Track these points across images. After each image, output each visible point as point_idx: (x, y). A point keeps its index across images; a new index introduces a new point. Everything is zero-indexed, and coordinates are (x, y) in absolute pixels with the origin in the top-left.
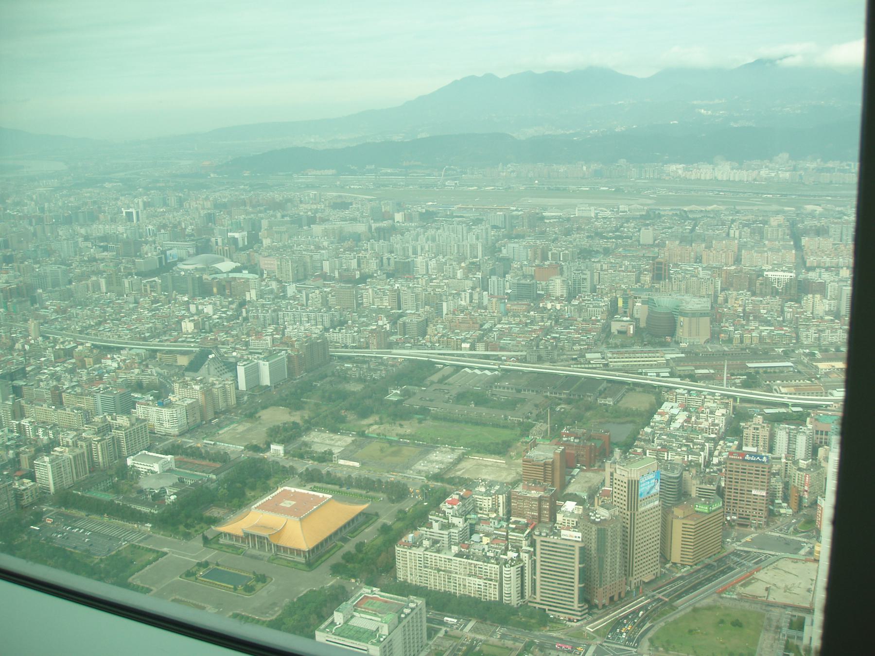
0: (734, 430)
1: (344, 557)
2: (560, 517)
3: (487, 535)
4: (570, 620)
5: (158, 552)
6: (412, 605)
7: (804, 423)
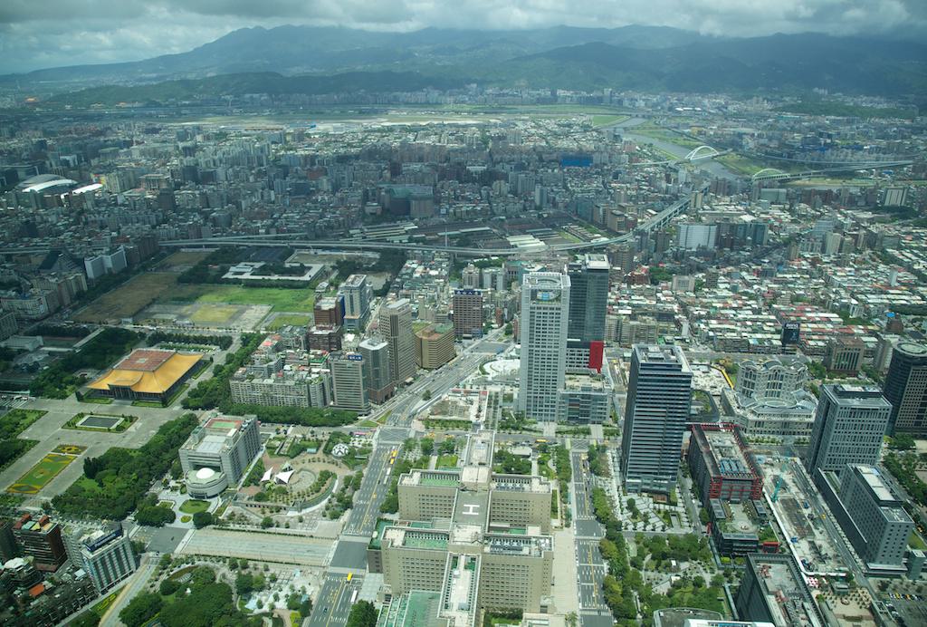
1: (189, 394)
3: (295, 364)
5: (39, 412)
7: (501, 266)
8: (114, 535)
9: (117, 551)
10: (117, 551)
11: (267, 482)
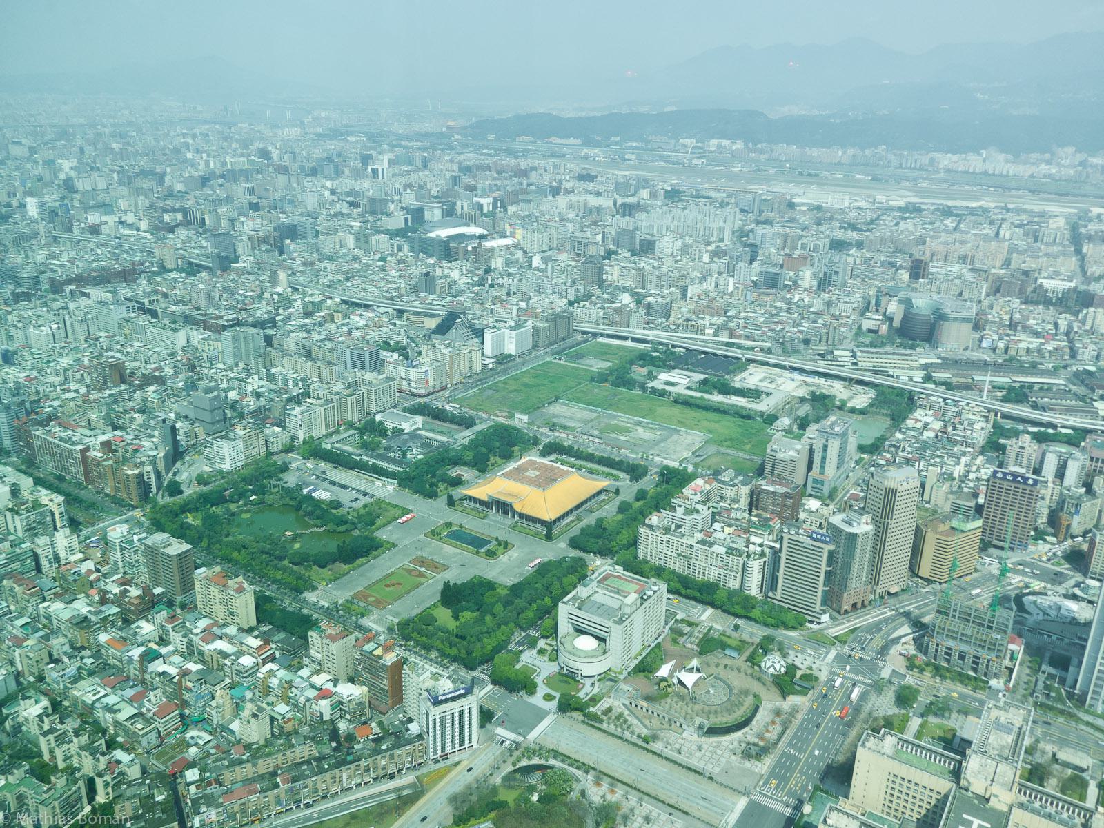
0: (994, 447)
1: (582, 530)
2: (802, 516)
3: (730, 526)
4: (811, 622)
6: (655, 588)
8: (463, 691)
9: (461, 713)
10: (461, 713)
11: (664, 679)
